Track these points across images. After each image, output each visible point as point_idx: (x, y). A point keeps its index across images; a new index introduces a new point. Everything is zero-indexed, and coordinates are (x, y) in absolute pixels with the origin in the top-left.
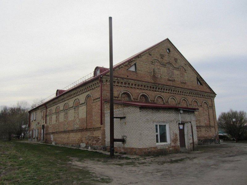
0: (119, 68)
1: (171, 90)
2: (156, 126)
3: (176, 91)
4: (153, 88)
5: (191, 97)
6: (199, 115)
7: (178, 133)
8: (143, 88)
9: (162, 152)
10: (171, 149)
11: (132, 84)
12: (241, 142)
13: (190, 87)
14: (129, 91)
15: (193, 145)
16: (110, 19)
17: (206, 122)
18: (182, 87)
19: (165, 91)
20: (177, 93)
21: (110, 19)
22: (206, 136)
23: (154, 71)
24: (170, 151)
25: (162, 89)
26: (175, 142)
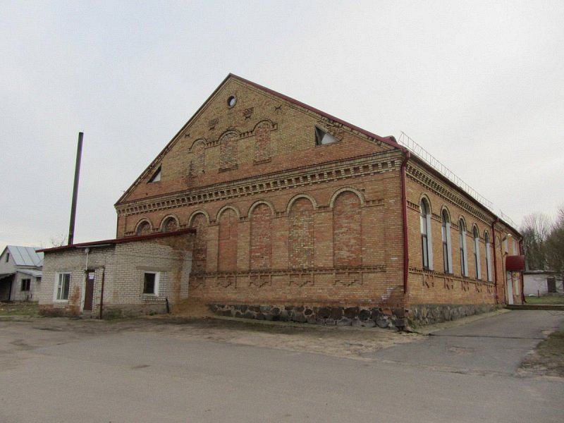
0: (137, 186)
1: (222, 192)
2: (61, 275)
3: (235, 190)
4: (183, 200)
5: (285, 192)
6: (313, 237)
7: (33, 285)
8: (166, 206)
9: (120, 312)
10: (68, 310)
11: (158, 204)
12: (304, 331)
13: (285, 165)
14: (173, 213)
15: (101, 308)
16: (81, 135)
17: (348, 254)
18: (257, 173)
19: (208, 199)
20: (238, 193)
21: (81, 135)
22: (336, 298)
23: (191, 166)
24: (66, 313)
25: (199, 197)
26: (75, 301)
